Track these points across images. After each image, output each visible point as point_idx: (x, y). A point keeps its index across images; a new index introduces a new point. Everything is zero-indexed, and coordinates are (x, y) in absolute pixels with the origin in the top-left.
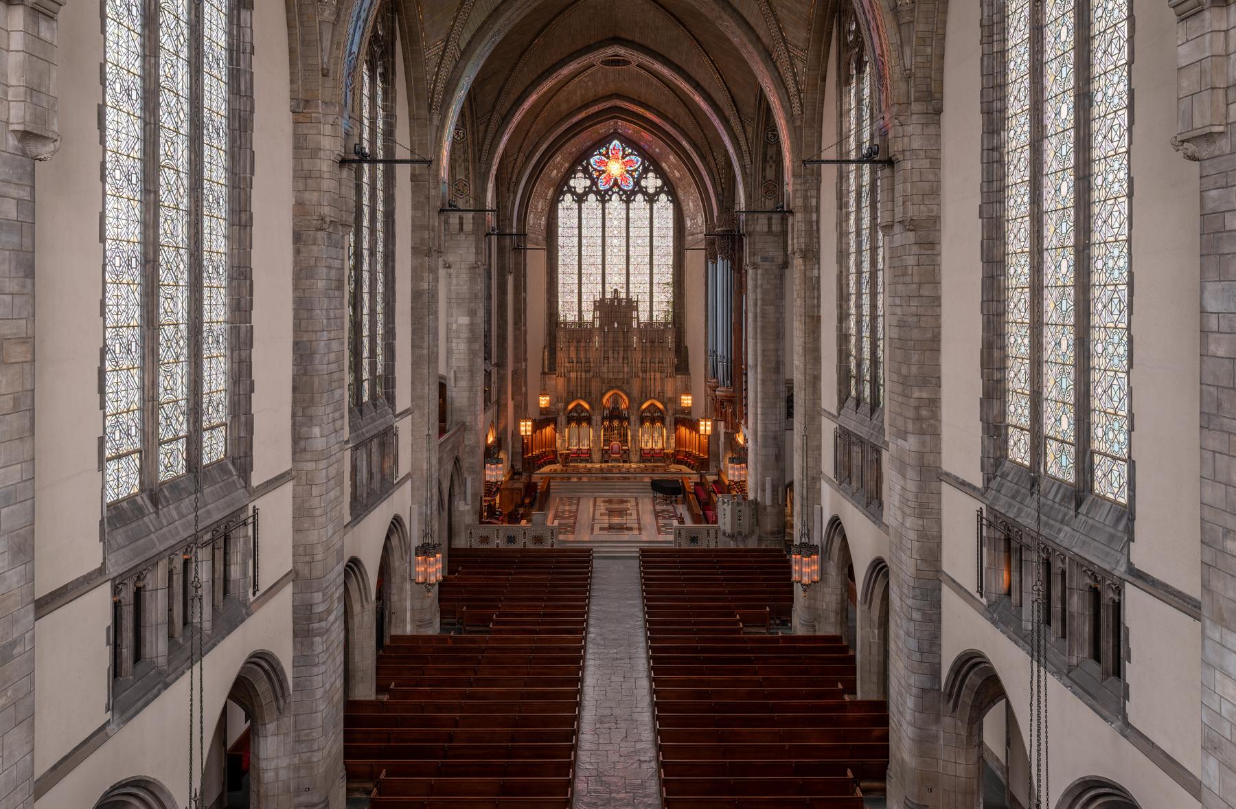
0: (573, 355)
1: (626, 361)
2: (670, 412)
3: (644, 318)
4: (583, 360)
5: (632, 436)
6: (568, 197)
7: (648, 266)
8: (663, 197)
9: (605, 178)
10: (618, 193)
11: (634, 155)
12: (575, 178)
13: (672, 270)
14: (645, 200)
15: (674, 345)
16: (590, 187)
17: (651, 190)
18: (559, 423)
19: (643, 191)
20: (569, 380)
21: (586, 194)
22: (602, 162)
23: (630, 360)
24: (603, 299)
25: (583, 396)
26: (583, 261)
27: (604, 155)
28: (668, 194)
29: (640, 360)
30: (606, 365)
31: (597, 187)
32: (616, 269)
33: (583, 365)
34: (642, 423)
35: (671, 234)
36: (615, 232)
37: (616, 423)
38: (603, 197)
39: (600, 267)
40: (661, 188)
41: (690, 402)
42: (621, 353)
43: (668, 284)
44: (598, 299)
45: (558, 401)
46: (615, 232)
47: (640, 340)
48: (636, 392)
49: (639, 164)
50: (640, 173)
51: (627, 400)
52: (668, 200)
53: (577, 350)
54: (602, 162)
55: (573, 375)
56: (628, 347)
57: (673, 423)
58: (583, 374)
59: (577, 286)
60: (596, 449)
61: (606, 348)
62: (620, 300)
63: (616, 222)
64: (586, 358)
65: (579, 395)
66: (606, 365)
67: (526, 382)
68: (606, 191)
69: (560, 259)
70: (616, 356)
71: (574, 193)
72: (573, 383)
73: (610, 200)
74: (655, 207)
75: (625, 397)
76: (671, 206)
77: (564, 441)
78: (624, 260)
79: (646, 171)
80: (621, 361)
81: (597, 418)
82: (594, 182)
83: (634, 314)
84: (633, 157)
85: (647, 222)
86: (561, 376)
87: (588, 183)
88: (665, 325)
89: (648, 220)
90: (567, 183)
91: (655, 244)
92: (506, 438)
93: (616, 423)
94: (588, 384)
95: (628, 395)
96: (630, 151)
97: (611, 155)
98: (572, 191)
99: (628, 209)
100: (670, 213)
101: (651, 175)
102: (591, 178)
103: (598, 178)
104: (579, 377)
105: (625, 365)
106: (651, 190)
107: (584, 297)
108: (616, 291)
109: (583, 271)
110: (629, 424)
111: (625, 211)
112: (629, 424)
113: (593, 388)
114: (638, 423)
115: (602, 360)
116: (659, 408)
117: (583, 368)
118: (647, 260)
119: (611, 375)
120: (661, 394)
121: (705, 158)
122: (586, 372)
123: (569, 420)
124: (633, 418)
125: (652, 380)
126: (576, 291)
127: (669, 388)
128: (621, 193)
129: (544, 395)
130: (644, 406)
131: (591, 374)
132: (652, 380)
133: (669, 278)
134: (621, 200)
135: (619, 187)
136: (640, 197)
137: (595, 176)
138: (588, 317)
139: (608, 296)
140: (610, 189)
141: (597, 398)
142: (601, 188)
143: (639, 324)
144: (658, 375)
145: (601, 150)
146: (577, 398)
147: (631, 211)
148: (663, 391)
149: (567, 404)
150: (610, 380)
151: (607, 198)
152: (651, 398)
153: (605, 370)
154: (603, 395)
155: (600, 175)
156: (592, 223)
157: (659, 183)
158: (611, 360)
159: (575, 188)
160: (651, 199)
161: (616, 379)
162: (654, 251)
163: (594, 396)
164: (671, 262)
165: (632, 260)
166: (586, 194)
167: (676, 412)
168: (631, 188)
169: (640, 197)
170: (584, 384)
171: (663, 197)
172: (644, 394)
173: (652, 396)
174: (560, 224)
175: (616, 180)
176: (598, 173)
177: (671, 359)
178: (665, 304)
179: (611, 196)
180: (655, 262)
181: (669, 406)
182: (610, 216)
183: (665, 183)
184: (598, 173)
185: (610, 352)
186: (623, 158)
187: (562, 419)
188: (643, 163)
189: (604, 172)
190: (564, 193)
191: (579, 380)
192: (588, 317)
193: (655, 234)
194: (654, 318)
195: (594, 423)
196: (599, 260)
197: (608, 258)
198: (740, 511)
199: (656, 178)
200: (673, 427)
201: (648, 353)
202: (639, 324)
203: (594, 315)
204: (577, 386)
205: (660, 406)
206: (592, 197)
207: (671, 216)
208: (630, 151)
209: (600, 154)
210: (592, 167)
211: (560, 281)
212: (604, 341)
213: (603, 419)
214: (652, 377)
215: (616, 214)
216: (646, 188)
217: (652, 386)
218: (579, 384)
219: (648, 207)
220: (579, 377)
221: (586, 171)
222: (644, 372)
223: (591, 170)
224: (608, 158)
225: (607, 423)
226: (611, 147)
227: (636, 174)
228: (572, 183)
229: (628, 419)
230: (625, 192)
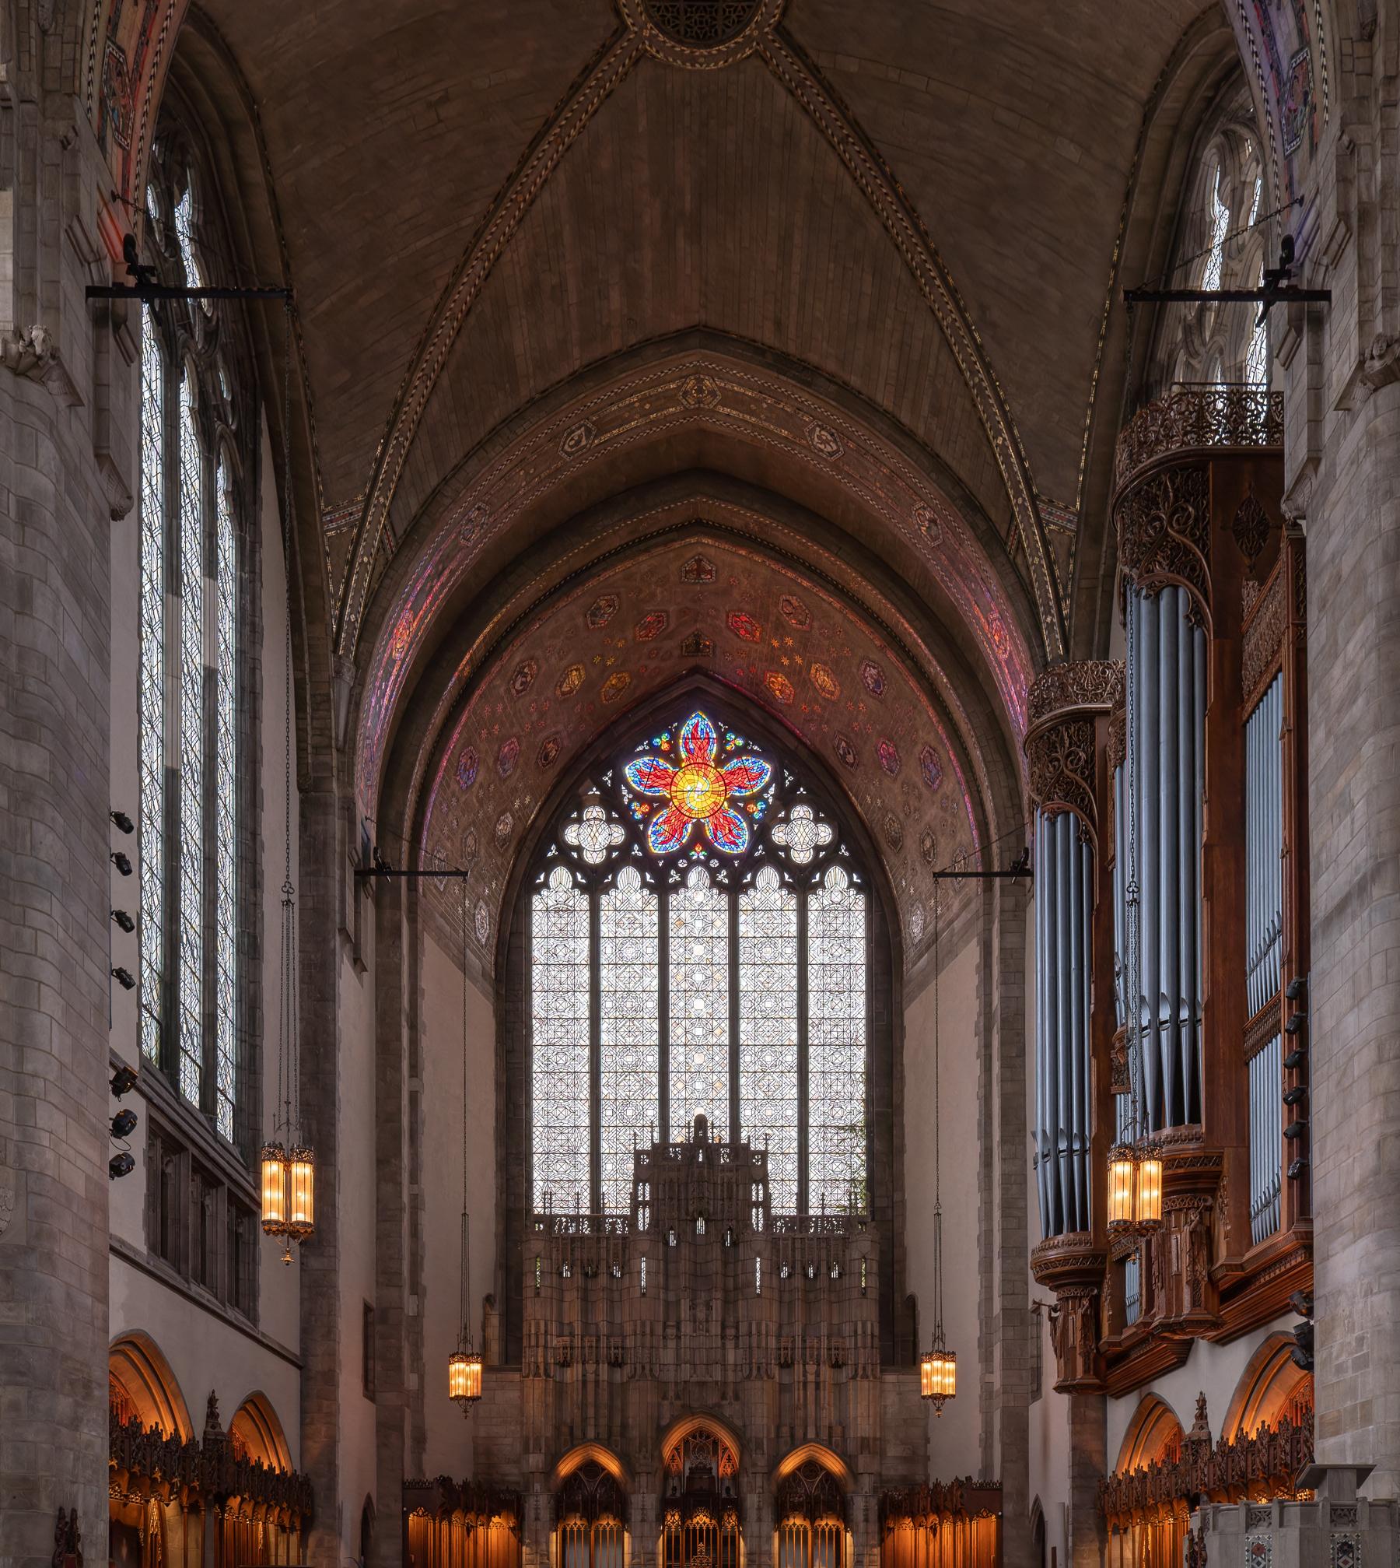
0: (573, 1313)
1: (731, 1332)
2: (867, 1482)
3: (784, 1202)
4: (604, 1328)
5: (750, 1554)
6: (561, 877)
7: (793, 1078)
8: (837, 876)
9: (667, 821)
10: (705, 864)
11: (753, 753)
12: (579, 821)
13: (862, 1087)
14: (783, 884)
15: (874, 1282)
16: (625, 849)
17: (802, 857)
18: (530, 1514)
19: (779, 858)
20: (560, 1389)
21: (612, 866)
22: (658, 775)
23: (743, 1329)
24: (661, 1149)
25: (604, 1435)
26: (606, 1061)
27: (665, 755)
28: (849, 867)
29: (773, 1327)
30: (672, 1344)
31: (644, 848)
32: (699, 1086)
33: (603, 1343)
34: (780, 1514)
35: (860, 981)
36: (699, 977)
37: (702, 1519)
38: (661, 876)
39: (655, 1079)
40: (832, 849)
41: (951, 1380)
42: (717, 1305)
44: (648, 1146)
45: (526, 1451)
46: (699, 977)
47: (773, 1270)
48: (761, 1420)
49: (767, 778)
50: (769, 808)
52: (851, 884)
53: (585, 1299)
54: (658, 775)
55: (572, 1374)
56: (735, 1290)
57: (873, 1516)
58: (604, 1369)
59: (586, 1134)
61: (672, 1297)
62: (712, 1151)
63: (698, 950)
64: (611, 1323)
65: (591, 1434)
66: (672, 1344)
67: (417, 1357)
68: (671, 860)
69: (537, 1054)
70: (701, 1315)
71: (576, 865)
73: (682, 884)
74: (813, 903)
75: (728, 1440)
76: (860, 902)
78: (722, 1057)
79: (786, 799)
80: (715, 1329)
81: (644, 1501)
82: (635, 834)
83: (757, 1193)
84: (748, 762)
85: (790, 950)
86: (537, 1375)
87: (618, 835)
88: (849, 1221)
89: (794, 943)
90: (556, 837)
91: (813, 1011)
92: (332, 1487)
93: (702, 1519)
94: (618, 1403)
95: (738, 1434)
96: (740, 742)
97: (684, 755)
98: (571, 858)
99: (734, 911)
100: (858, 924)
101: (801, 811)
102: (624, 818)
103: (646, 820)
104: (591, 1377)
105: (730, 1344)
106: (802, 857)
107: (608, 1168)
108: (701, 1122)
109: (604, 1091)
110: (741, 1520)
111: (725, 916)
112: (741, 1520)
114: (768, 1515)
115: (659, 1330)
116: (829, 1475)
117: (603, 1352)
118: (791, 1058)
119: (686, 1373)
120: (838, 1430)
121: (1003, 544)
122: (616, 1364)
123: (560, 1512)
124: (752, 1501)
125: (811, 1388)
126: (585, 1149)
128: (714, 863)
129: (467, 1358)
130: (788, 1466)
131: (627, 1369)
132: (811, 1388)
133: (855, 1112)
134: (715, 883)
135: (707, 846)
136: (768, 877)
137: (638, 816)
139: (677, 1136)
140: (684, 852)
142: (656, 850)
143: (770, 1220)
144: (826, 1372)
145: (657, 741)
146: (584, 1441)
147: (742, 918)
149: (554, 1459)
151: (674, 877)
152: (805, 1441)
153: (668, 1356)
154: (662, 1432)
155: (653, 812)
156: (629, 952)
157: (825, 834)
158: (687, 1328)
159: (579, 849)
161: (702, 1384)
162: (812, 1032)
163: (634, 1433)
164: (860, 1066)
165: (746, 1059)
166: (612, 866)
167: (881, 1480)
168: (742, 849)
169: (768, 877)
170: (604, 1397)
171: (837, 876)
172: (785, 1430)
173: (811, 1434)
174: (536, 954)
175: (699, 827)
176: (645, 808)
177: (865, 1315)
178: (844, 1186)
179: (684, 873)
180: (814, 1065)
181: (863, 1462)
182: (683, 932)
183: (840, 836)
184: (645, 808)
185: (685, 1305)
186: (720, 762)
187: (539, 1503)
188: (778, 778)
189: (664, 802)
190: (549, 866)
191: (591, 1387)
192: (617, 1198)
193: (813, 983)
194: (813, 1200)
195: (635, 1516)
196: (652, 1060)
197: (677, 1055)
198: (1346, 1548)
199: (817, 820)
200: (874, 1527)
201: (798, 1307)
202: (770, 1220)
203: (634, 1196)
204: (584, 1406)
205: (833, 1464)
206: (629, 877)
207: (861, 932)
208: (740, 742)
209: (655, 751)
210: (630, 790)
211: (538, 1120)
212: (666, 1262)
213: (666, 1504)
214: (811, 1378)
215: (699, 924)
216: (787, 849)
217: (811, 1408)
218: (591, 1399)
219: (793, 903)
220: (591, 1377)
221: (611, 801)
222: (786, 1365)
224: (676, 762)
225: (673, 1519)
226: (685, 730)
227: (757, 810)
228: (571, 835)
229: (737, 1505)
230: (726, 861)
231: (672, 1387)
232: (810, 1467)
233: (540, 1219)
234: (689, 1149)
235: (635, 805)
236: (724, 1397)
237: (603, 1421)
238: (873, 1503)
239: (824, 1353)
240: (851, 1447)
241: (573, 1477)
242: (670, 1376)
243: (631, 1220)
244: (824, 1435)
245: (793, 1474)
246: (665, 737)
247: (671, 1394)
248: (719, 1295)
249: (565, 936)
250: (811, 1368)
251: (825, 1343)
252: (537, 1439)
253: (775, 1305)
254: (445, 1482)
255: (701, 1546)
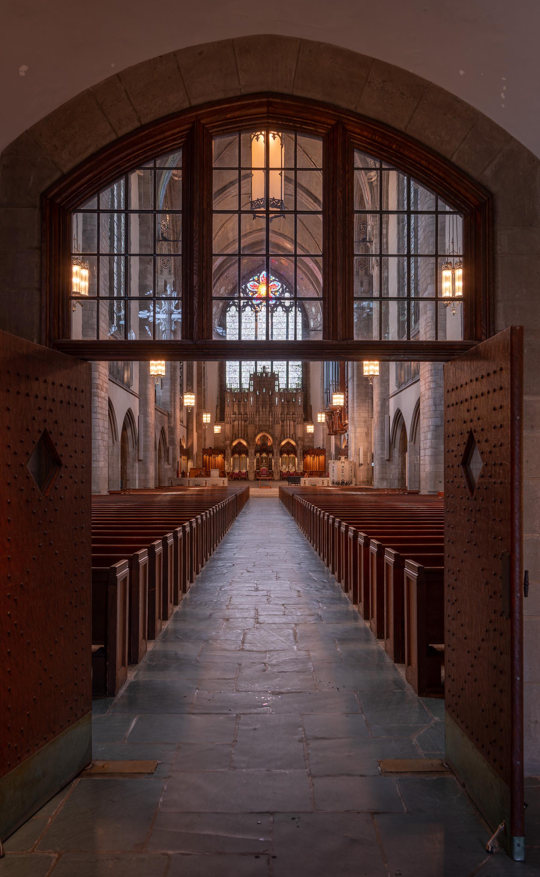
1: (271, 414)
2: (300, 447)
4: (243, 413)
5: (275, 463)
18: (227, 454)
20: (233, 426)
22: (255, 286)
23: (273, 413)
25: (243, 436)
27: (256, 281)
29: (280, 413)
30: (258, 416)
33: (243, 416)
34: (281, 453)
37: (264, 455)
43: (299, 366)
47: (280, 400)
49: (279, 287)
51: (271, 440)
55: (236, 423)
56: (272, 404)
57: (301, 454)
60: (252, 471)
62: (267, 374)
65: (240, 436)
72: (236, 428)
75: (270, 438)
77: (230, 466)
80: (267, 413)
81: (252, 451)
83: (276, 383)
84: (275, 283)
86: (228, 423)
88: (296, 389)
93: (264, 455)
95: (272, 436)
96: (274, 278)
97: (261, 281)
104: (240, 424)
105: (270, 416)
107: (243, 375)
110: (273, 455)
112: (273, 455)
113: (249, 431)
114: (279, 454)
115: (255, 413)
116: (292, 445)
117: (243, 418)
119: (261, 423)
120: (294, 435)
122: (245, 421)
123: (233, 453)
124: (275, 451)
125: (288, 426)
126: (238, 370)
127: (299, 431)
130: (283, 443)
131: (248, 422)
132: (288, 426)
136: (280, 309)
138: (246, 386)
141: (251, 438)
143: (279, 389)
144: (292, 423)
145: (254, 278)
148: (295, 433)
149: (232, 442)
150: (260, 426)
152: (287, 438)
153: (257, 419)
154: (256, 436)
158: (261, 413)
160: (287, 310)
163: (249, 436)
167: (304, 446)
173: (288, 436)
174: (227, 326)
181: (299, 442)
182: (260, 321)
185: (261, 408)
187: (229, 451)
188: (282, 287)
190: (230, 306)
191: (240, 426)
195: (250, 454)
200: (302, 457)
202: (279, 389)
205: (293, 443)
209: (254, 280)
210: (249, 290)
212: (257, 398)
213: (256, 452)
214: (288, 424)
219: (285, 315)
220: (240, 424)
223: (248, 291)
224: (259, 283)
229: (272, 452)
231: (258, 426)
232: (288, 443)
233: (228, 389)
234: (262, 374)
235: (249, 293)
236: (269, 428)
237: (243, 434)
238: (302, 452)
239: (291, 418)
240: (297, 439)
241: (236, 445)
242: (257, 423)
243: (249, 389)
244: (291, 436)
245: (284, 445)
246: (256, 277)
247: (258, 427)
248: (268, 406)
249: (234, 322)
250: (288, 422)
251: (291, 417)
252: (228, 438)
253: (281, 408)
254: (210, 448)
255: (264, 461)
